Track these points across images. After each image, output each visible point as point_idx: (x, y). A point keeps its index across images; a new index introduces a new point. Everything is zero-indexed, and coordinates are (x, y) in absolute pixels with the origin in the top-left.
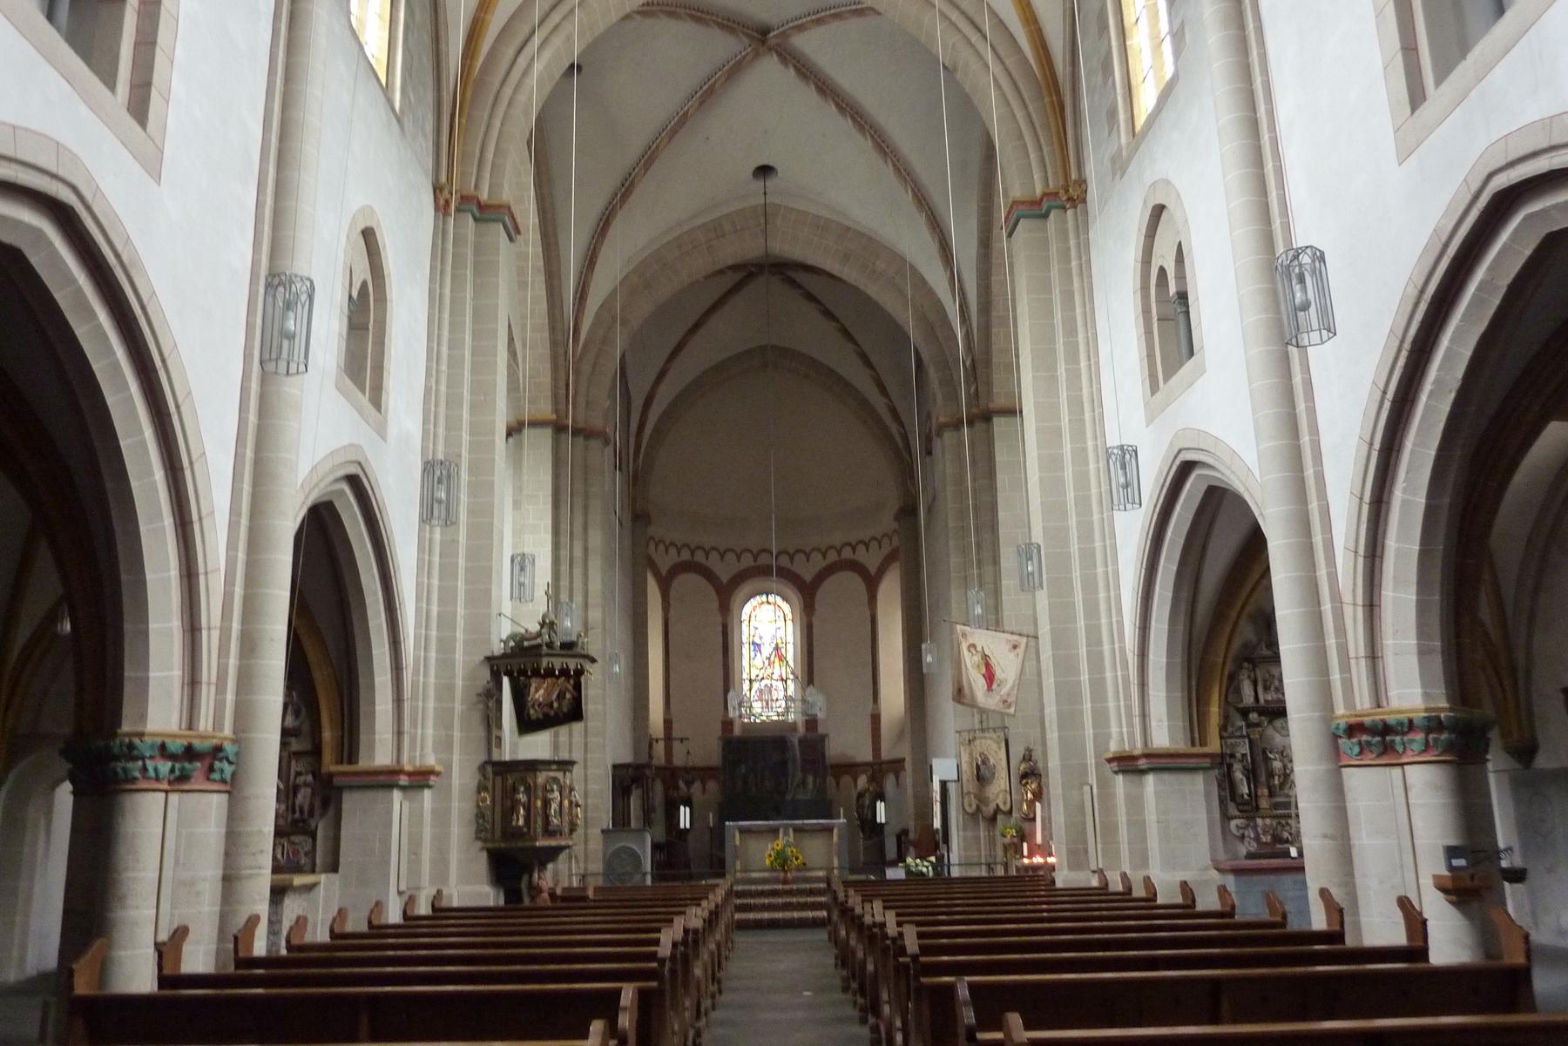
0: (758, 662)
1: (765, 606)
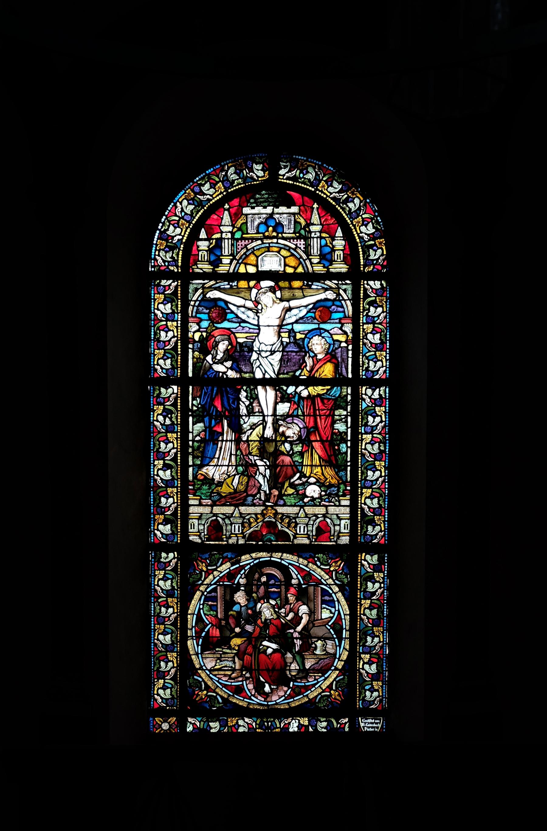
0: (220, 468)
1: (256, 213)
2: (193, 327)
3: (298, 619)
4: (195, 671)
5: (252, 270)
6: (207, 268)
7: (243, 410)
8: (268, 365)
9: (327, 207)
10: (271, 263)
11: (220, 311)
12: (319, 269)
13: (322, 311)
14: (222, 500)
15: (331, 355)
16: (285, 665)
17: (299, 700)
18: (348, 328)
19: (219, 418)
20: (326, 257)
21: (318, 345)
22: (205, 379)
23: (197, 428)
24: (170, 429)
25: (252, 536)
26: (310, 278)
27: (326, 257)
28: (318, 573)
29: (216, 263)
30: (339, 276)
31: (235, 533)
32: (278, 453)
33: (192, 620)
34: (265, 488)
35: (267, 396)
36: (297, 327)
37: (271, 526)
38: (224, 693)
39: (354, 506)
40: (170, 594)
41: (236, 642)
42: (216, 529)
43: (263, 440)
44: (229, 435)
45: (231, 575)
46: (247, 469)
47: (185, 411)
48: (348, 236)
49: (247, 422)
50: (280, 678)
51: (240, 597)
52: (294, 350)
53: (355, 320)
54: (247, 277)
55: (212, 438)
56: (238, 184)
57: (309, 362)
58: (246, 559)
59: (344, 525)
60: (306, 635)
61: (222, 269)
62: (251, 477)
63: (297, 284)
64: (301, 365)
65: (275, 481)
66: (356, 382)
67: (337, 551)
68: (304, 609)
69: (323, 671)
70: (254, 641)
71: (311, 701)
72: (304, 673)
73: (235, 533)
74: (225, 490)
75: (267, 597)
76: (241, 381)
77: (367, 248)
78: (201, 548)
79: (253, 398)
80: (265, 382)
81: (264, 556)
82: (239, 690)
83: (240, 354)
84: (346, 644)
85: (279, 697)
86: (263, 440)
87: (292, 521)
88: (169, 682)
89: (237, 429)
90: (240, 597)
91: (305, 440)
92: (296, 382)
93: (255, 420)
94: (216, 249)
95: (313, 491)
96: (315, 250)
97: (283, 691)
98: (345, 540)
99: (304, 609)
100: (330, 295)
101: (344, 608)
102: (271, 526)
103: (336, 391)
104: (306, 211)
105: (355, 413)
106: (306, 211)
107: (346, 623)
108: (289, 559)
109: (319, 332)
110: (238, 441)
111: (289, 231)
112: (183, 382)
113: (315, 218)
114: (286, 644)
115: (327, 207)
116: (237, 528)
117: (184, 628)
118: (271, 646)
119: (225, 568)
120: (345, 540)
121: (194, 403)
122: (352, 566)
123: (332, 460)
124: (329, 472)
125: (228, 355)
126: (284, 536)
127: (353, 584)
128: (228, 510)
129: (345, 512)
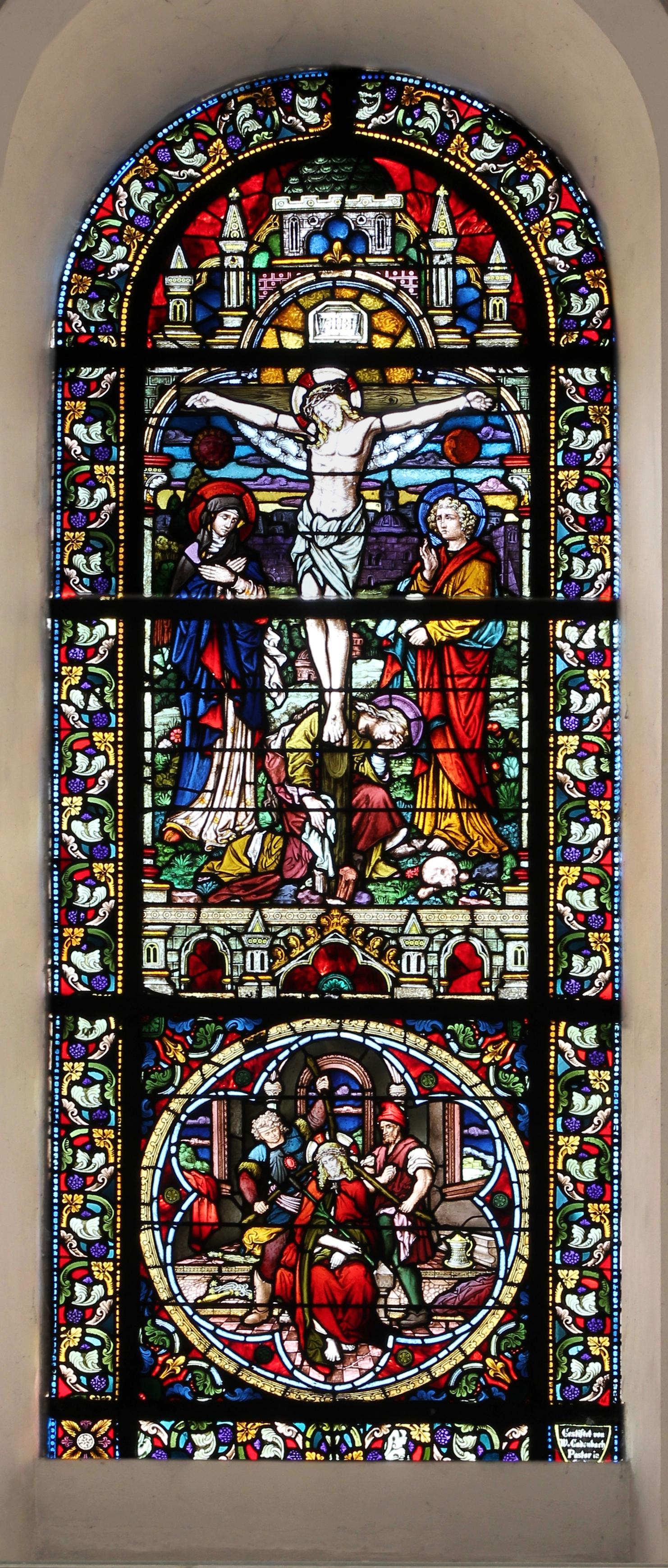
0: (219, 814)
1: (303, 207)
2: (157, 478)
3: (404, 1183)
4: (157, 1308)
5: (292, 342)
6: (188, 338)
7: (272, 676)
8: (331, 569)
9: (468, 197)
10: (338, 326)
11: (216, 439)
12: (450, 339)
13: (459, 440)
14: (224, 893)
15: (481, 544)
16: (374, 1295)
17: (409, 1382)
18: (521, 479)
19: (215, 695)
20: (468, 312)
21: (449, 520)
22: (182, 603)
23: (162, 720)
24: (98, 721)
25: (296, 979)
26: (428, 361)
27: (468, 312)
28: (455, 1069)
29: (208, 323)
30: (499, 357)
31: (252, 973)
32: (355, 780)
33: (149, 1183)
34: (325, 862)
35: (328, 643)
36: (401, 477)
37: (338, 956)
38: (229, 1361)
39: (538, 909)
40: (97, 1118)
41: (258, 1235)
42: (206, 961)
43: (320, 748)
44: (238, 736)
45: (246, 1073)
46: (286, 819)
47: (136, 681)
48: (519, 262)
49: (282, 706)
50: (362, 1324)
51: (266, 1127)
52: (393, 531)
53: (537, 460)
54: (282, 358)
55: (199, 740)
56: (261, 141)
57: (430, 560)
58: (279, 1034)
59: (515, 955)
60: (425, 1222)
61: (222, 341)
62: (291, 836)
63: (399, 375)
64: (412, 568)
65: (351, 847)
66: (541, 612)
67: (497, 1015)
68: (419, 1157)
69: (467, 1309)
70: (296, 1233)
71: (439, 1384)
72: (423, 1313)
73: (252, 973)
74: (229, 867)
75: (330, 1127)
76: (270, 609)
77: (563, 291)
78: (173, 1007)
79: (297, 647)
80: (323, 610)
81: (321, 1026)
82: (263, 1355)
83: (266, 543)
84: (522, 1244)
85: (359, 1373)
86: (320, 748)
87: (390, 943)
88: (96, 1335)
89: (259, 723)
90: (266, 1127)
91: (419, 749)
92: (400, 610)
93: (298, 700)
94: (208, 298)
95: (439, 871)
96: (442, 296)
97: (369, 1358)
98: (517, 990)
99: (419, 1157)
100: (477, 401)
101: (518, 1157)
102: (338, 956)
103: (493, 633)
104: (420, 205)
105: (539, 685)
106: (420, 205)
107: (522, 1193)
108: (382, 1034)
109: (452, 488)
110: (260, 750)
111: (380, 251)
112: (131, 612)
113: (442, 221)
114: (377, 1246)
115: (468, 197)
116: (257, 962)
117: (131, 1203)
118: (341, 1248)
119: (231, 1055)
120: (517, 990)
121: (156, 661)
122: (535, 1053)
123: (483, 794)
124: (478, 826)
125: (237, 542)
126: (373, 980)
127: (536, 1099)
128: (237, 916)
129: (516, 920)
